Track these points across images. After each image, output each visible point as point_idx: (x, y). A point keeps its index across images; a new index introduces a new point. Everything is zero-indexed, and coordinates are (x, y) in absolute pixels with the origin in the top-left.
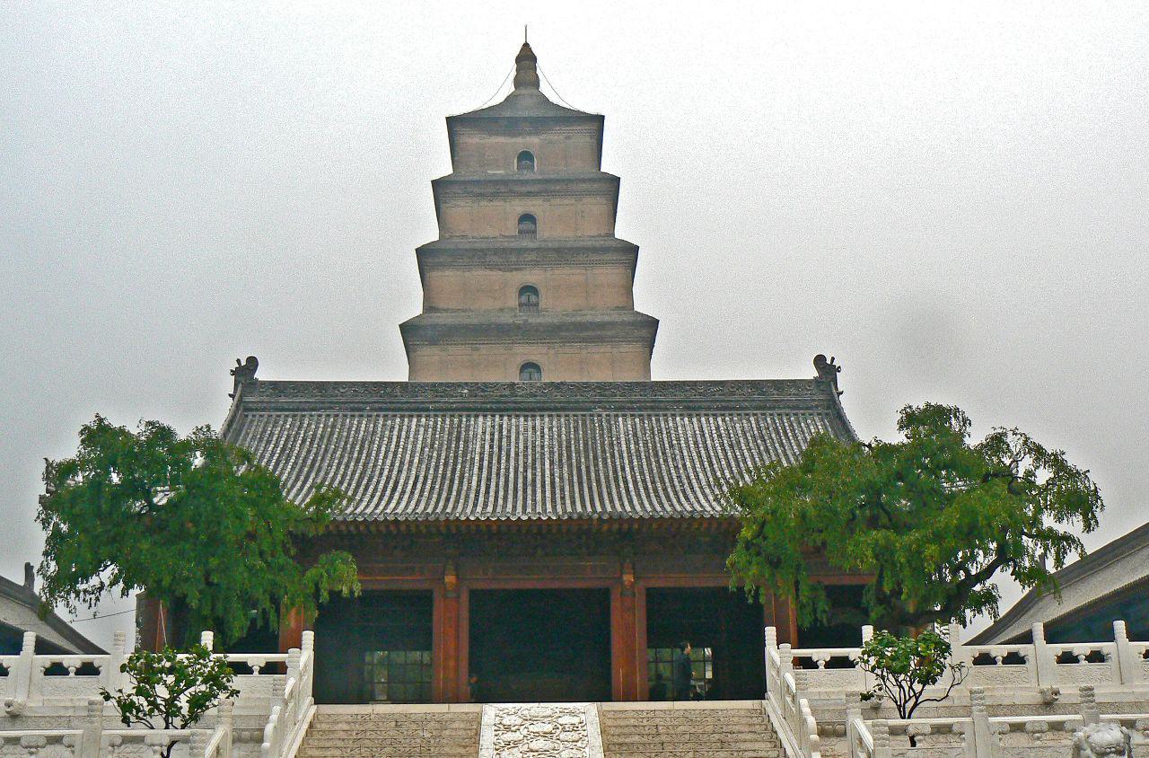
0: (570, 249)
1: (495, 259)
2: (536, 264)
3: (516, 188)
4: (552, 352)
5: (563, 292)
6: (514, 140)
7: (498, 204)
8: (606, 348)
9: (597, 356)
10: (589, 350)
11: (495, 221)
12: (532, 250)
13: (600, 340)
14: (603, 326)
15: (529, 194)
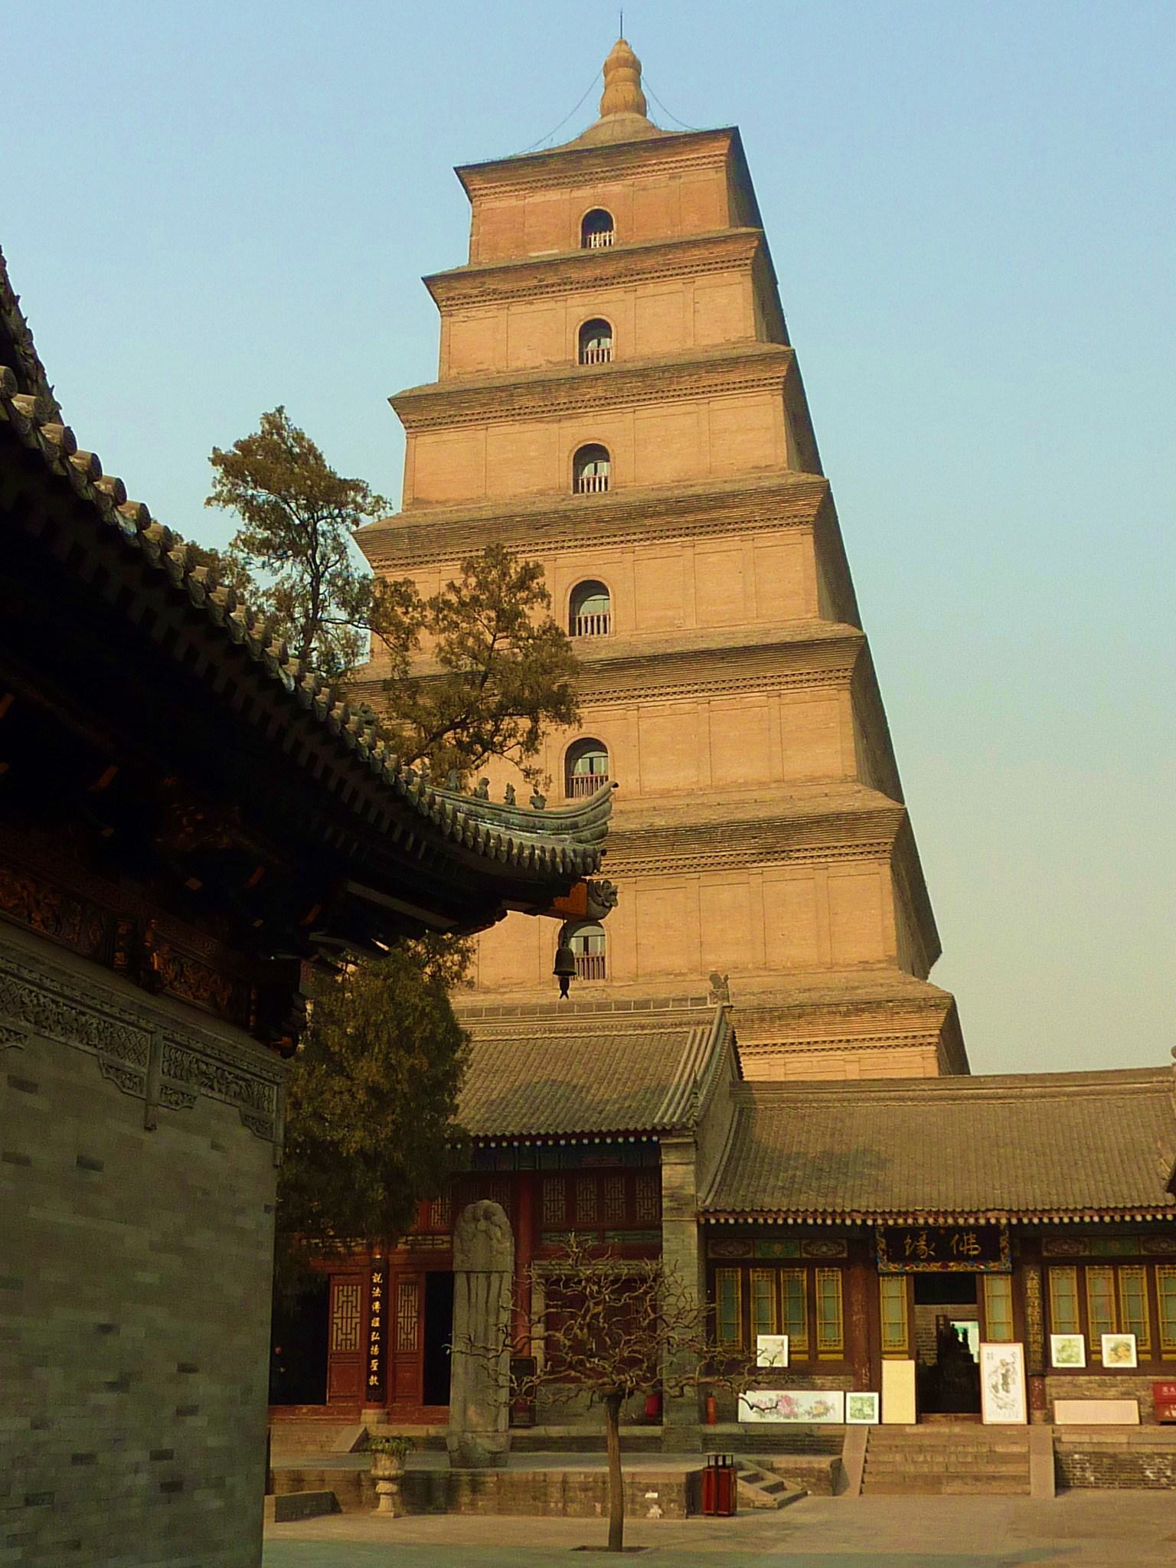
0: (666, 369)
1: (527, 401)
2: (605, 402)
3: (575, 275)
4: (630, 557)
5: (660, 447)
6: (577, 193)
7: (546, 306)
8: (732, 542)
9: (714, 558)
10: (698, 550)
11: (534, 335)
12: (596, 378)
13: (717, 528)
14: (722, 501)
15: (599, 283)
